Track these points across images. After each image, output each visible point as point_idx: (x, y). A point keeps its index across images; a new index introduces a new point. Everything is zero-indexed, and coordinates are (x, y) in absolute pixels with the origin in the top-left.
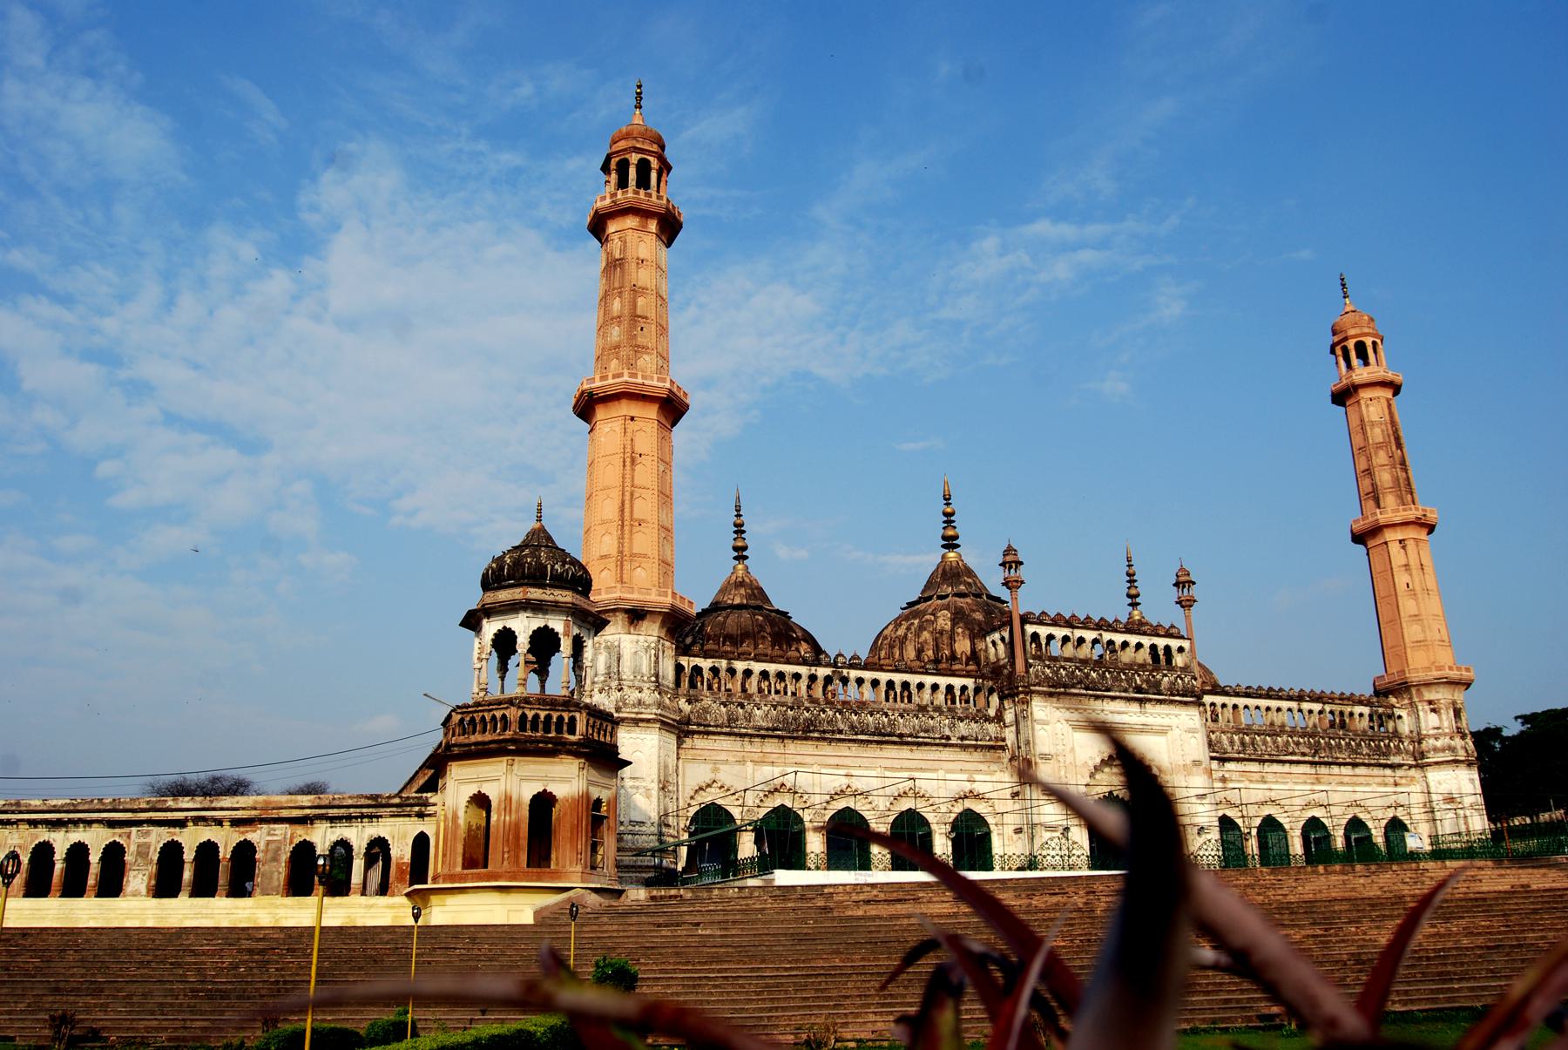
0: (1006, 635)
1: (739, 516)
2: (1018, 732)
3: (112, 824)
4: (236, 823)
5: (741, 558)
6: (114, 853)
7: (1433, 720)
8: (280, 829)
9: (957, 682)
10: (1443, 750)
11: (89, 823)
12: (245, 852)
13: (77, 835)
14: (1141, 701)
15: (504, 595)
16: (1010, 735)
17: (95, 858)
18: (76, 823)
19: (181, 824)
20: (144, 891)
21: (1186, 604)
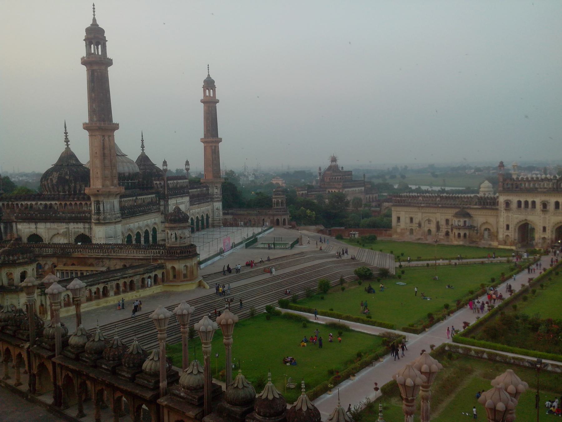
0: (162, 183)
1: (66, 130)
2: (165, 208)
3: (104, 282)
4: (130, 277)
5: (68, 145)
6: (105, 289)
7: (216, 191)
8: (138, 277)
9: (154, 196)
10: (217, 198)
11: (99, 284)
12: (132, 282)
13: (96, 286)
14: (182, 197)
15: (182, 225)
16: (162, 208)
17: (101, 290)
18: (96, 284)
19: (118, 280)
20: (113, 294)
21: (187, 170)
